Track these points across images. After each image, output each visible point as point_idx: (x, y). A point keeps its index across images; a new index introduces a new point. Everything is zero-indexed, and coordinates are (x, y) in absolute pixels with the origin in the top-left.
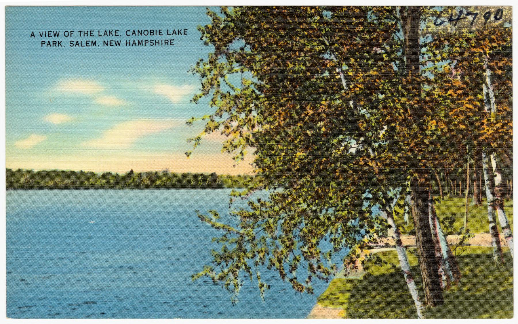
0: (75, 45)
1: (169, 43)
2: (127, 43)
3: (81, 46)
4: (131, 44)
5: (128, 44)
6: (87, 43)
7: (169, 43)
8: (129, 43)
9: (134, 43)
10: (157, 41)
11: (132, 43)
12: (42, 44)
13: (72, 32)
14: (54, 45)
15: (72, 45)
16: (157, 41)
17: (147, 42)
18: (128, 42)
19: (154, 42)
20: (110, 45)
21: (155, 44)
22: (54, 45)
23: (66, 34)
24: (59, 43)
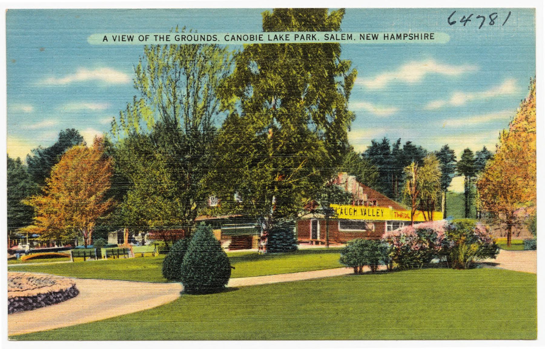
0: (330, 38)
1: (429, 37)
2: (385, 37)
3: (337, 40)
4: (396, 39)
5: (386, 38)
6: (342, 37)
7: (429, 37)
8: (388, 37)
9: (392, 37)
10: (416, 35)
11: (390, 37)
12: (295, 37)
13: (147, 37)
14: (308, 38)
15: (327, 38)
16: (416, 35)
17: (405, 35)
18: (386, 35)
19: (413, 36)
20: (367, 39)
21: (414, 37)
22: (308, 38)
23: (141, 38)
24: (313, 37)
